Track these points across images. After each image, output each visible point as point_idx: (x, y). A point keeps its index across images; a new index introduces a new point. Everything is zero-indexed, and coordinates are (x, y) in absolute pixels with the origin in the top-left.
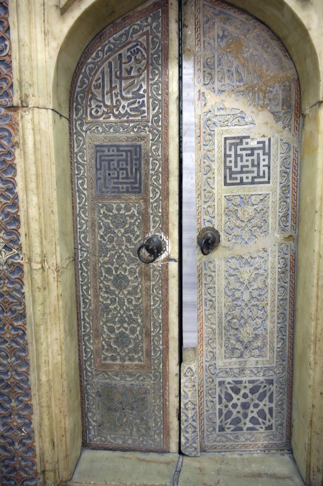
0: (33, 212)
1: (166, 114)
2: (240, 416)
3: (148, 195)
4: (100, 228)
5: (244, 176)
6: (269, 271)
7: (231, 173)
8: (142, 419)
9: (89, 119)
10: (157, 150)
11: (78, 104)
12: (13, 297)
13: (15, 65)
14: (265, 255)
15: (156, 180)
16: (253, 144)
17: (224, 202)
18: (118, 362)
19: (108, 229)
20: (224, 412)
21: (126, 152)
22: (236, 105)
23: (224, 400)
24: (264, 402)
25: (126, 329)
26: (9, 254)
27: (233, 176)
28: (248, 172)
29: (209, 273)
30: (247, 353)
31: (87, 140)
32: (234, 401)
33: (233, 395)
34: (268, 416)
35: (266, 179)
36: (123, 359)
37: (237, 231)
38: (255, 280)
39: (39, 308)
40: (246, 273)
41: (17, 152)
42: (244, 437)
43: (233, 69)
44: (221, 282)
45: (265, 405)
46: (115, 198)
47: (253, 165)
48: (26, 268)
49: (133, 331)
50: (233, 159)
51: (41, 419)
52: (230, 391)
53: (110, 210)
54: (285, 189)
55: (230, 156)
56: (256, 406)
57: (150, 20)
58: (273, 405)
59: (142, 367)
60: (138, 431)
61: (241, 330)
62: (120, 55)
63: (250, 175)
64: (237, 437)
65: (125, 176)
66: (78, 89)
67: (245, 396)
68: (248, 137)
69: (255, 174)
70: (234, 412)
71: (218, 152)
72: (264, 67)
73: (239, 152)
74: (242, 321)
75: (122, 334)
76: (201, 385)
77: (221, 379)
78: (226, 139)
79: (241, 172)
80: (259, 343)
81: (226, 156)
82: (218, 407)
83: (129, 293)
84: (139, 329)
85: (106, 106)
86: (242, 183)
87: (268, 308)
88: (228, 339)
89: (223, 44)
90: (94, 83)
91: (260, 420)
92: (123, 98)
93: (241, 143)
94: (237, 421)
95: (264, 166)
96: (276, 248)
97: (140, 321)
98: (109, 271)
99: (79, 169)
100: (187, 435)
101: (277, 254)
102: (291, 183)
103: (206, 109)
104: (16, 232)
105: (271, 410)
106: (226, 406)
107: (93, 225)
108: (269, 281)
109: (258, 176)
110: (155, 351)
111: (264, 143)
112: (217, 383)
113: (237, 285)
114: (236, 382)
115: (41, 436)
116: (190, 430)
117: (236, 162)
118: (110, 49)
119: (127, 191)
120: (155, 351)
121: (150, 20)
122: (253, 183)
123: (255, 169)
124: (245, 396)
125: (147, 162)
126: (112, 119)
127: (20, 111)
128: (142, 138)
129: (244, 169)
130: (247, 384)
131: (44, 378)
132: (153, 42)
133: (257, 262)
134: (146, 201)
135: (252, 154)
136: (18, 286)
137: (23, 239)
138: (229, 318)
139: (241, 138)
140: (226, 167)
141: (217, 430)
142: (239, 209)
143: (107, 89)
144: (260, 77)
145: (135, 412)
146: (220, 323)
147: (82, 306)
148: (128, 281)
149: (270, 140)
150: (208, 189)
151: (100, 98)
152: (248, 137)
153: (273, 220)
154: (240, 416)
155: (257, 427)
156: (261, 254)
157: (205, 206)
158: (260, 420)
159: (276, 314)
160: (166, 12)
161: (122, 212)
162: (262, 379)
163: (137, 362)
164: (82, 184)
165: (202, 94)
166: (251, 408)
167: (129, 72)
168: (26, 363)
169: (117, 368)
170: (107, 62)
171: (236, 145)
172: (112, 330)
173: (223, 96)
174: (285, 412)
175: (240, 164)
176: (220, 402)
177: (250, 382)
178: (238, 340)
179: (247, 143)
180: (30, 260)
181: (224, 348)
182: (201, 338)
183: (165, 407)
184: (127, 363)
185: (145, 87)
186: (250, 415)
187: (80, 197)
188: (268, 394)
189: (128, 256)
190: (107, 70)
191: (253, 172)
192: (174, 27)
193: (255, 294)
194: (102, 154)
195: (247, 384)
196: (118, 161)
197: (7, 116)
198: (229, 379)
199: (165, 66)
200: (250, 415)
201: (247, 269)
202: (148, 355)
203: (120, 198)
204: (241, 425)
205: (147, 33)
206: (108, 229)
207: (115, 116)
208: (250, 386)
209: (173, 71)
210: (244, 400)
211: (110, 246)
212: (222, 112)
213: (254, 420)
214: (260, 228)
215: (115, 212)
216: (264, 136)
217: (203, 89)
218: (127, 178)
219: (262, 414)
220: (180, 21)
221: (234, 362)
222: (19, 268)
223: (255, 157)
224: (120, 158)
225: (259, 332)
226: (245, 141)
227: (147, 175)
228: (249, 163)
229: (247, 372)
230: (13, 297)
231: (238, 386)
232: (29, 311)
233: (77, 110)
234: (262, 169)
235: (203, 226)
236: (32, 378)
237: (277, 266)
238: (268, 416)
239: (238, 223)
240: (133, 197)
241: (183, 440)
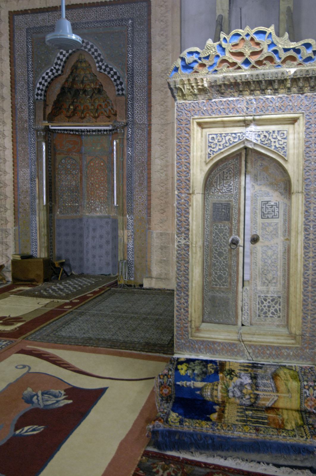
0: (194, 227)
1: (240, 193)
2: (267, 311)
3: (232, 221)
4: (213, 233)
5: (269, 215)
6: (279, 252)
7: (264, 214)
8: (227, 311)
9: (211, 193)
10: (236, 205)
11: (208, 188)
12: (185, 256)
13: (191, 181)
14: (277, 245)
15: (236, 216)
16: (272, 204)
17: (261, 224)
18: (218, 286)
19: (217, 234)
20: (260, 308)
21: (225, 205)
22: (266, 189)
23: (260, 304)
24: (277, 306)
25: (222, 273)
26: (185, 241)
29: (255, 252)
30: (270, 285)
31: (210, 201)
32: (265, 304)
33: (264, 302)
34: (279, 312)
35: (277, 217)
36: (220, 285)
37: (266, 236)
38: (273, 255)
39: (194, 260)
40: (270, 253)
41: (190, 208)
42: (269, 320)
43: (265, 177)
44: (259, 256)
45: (277, 307)
46: (220, 222)
47: (272, 211)
48: (190, 246)
49: (224, 274)
50: (264, 209)
51: (192, 300)
52: (263, 300)
53: (217, 227)
54: (285, 221)
55: (263, 208)
56: (274, 307)
57: (235, 160)
58: (281, 307)
59: (228, 289)
60: (225, 316)
61: (268, 275)
62: (224, 172)
63: (271, 215)
64: (265, 320)
66: (208, 183)
67: (269, 302)
68: (270, 201)
70: (264, 309)
71: (259, 206)
72: (277, 176)
73: (267, 207)
74: (268, 272)
75: (220, 275)
76: (251, 297)
77: (259, 295)
78: (262, 202)
79: (268, 214)
80: (275, 281)
81: (262, 208)
82: (258, 306)
83: (224, 259)
84: (227, 273)
85: (218, 189)
86: (268, 218)
87: (279, 267)
88: (262, 278)
89: (261, 168)
90: (214, 181)
91: (275, 313)
92: (224, 186)
93: (268, 203)
94: (265, 313)
96: (282, 243)
97: (227, 270)
98: (216, 250)
99: (207, 211)
100: (245, 317)
101: (282, 245)
102: (287, 219)
103: (255, 191)
104: (188, 234)
105: (280, 309)
106: (261, 306)
107: (211, 232)
108: (279, 256)
109: (275, 216)
110: (233, 282)
111: (276, 203)
112: (257, 296)
113: (266, 257)
114: (265, 296)
115: (191, 307)
116: (246, 314)
118: (220, 170)
119: (225, 220)
120: (233, 282)
121: (235, 160)
122: (272, 218)
123: (273, 213)
124: (269, 302)
125: (232, 210)
126: (220, 194)
127: (192, 195)
128: (231, 201)
130: (270, 298)
131: (194, 285)
132: (236, 167)
133: (274, 248)
134: (231, 224)
135: (272, 207)
136: (187, 252)
137: (190, 236)
138: (263, 270)
139: (268, 202)
140: (262, 212)
141: (257, 316)
142: (267, 227)
143: (218, 183)
144: (275, 180)
145: (224, 308)
146: (259, 272)
147: (205, 263)
148: (223, 254)
149: (279, 202)
150: (255, 220)
151: (215, 186)
152: (270, 201)
153: (280, 232)
154: (267, 311)
155: (274, 316)
156: (276, 245)
157: (254, 226)
158: (275, 313)
159: (281, 269)
160: (241, 158)
161: (222, 227)
162: (276, 296)
163: (225, 287)
164: (207, 217)
165: (253, 186)
166: (272, 308)
167: (227, 178)
168: (188, 279)
169: (217, 289)
170: (219, 174)
171: (266, 204)
172: (216, 273)
173: (261, 187)
174: (286, 311)
175: (267, 211)
176: (259, 304)
177: (271, 297)
178: (266, 279)
180: (192, 243)
181: (260, 282)
182: (251, 277)
183: (236, 306)
184: (222, 287)
185: (232, 183)
186: (271, 311)
187: (207, 222)
188: (279, 302)
189: (224, 244)
190: (219, 177)
192: (243, 163)
193: (273, 261)
195: (270, 298)
196: (222, 209)
197: (188, 196)
198: (263, 295)
199: (240, 175)
200: (271, 311)
201: (270, 251)
202: (230, 284)
203: (221, 222)
204: (267, 315)
205: (233, 165)
206: (217, 234)
207: (221, 193)
208: (271, 298)
209: (243, 178)
210: (268, 304)
211: (217, 240)
212: (261, 192)
213: (273, 313)
214: (275, 235)
215: (219, 227)
216: (277, 201)
217: (254, 184)
218: (225, 215)
219: (276, 310)
220: (246, 162)
221: (264, 288)
222: (188, 246)
223: (273, 209)
225: (275, 276)
226: (269, 202)
227: (232, 214)
228: (271, 211)
229: (270, 292)
230: (185, 256)
231: (266, 298)
232: (190, 261)
233: (207, 190)
235: (253, 234)
236: (190, 285)
237: (282, 250)
238: (279, 312)
239: (267, 233)
240: (227, 222)
241: (243, 319)
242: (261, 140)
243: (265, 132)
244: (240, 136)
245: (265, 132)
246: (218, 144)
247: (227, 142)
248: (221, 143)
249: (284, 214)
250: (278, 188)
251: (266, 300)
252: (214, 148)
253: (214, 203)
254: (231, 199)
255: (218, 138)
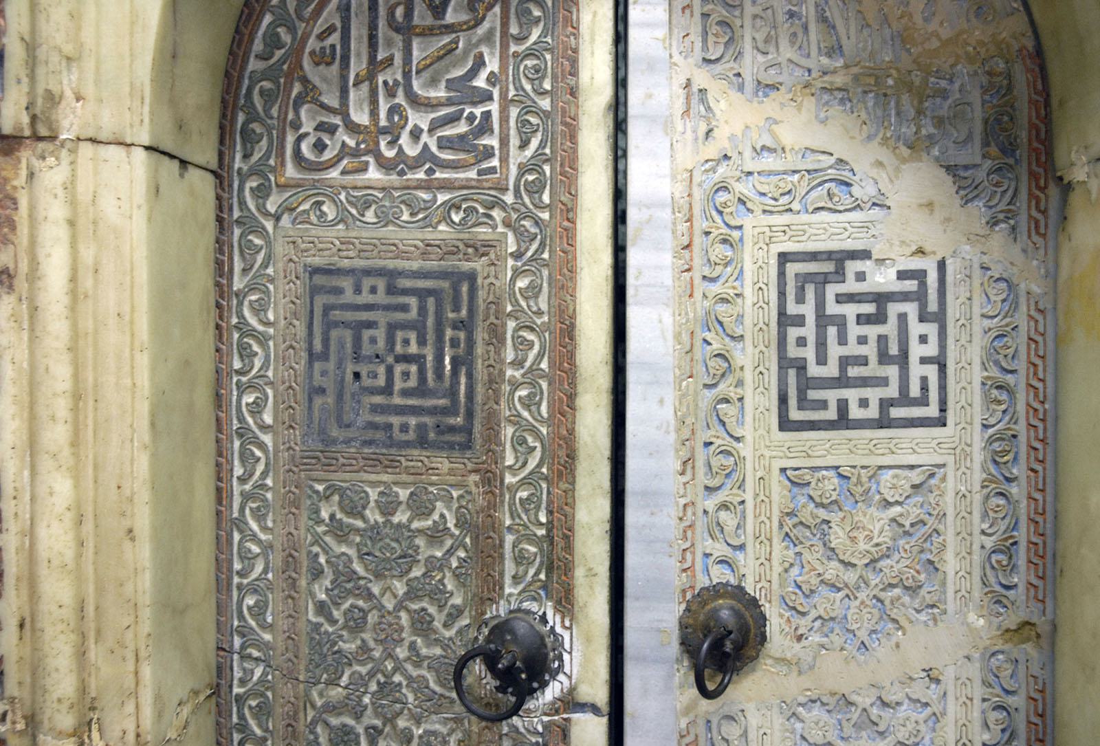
3: (498, 458)
4: (317, 573)
5: (852, 395)
7: (806, 383)
9: (291, 171)
10: (533, 292)
11: (253, 117)
14: (933, 693)
15: (528, 403)
16: (883, 279)
17: (778, 489)
19: (345, 581)
21: (422, 294)
22: (820, 138)
27: (813, 395)
28: (864, 382)
31: (280, 249)
35: (932, 411)
46: (375, 463)
47: (884, 358)
50: (809, 331)
53: (356, 511)
55: (800, 321)
63: (874, 395)
65: (413, 383)
66: (253, 65)
68: (865, 255)
69: (892, 391)
73: (832, 308)
78: (784, 258)
79: (842, 381)
81: (785, 320)
85: (352, 128)
86: (843, 421)
90: (312, 44)
92: (414, 100)
93: (840, 275)
95: (924, 361)
96: (974, 671)
99: (246, 353)
101: (978, 691)
102: (1021, 428)
107: (290, 561)
109: (904, 399)
111: (920, 275)
117: (821, 345)
119: (422, 442)
122: (883, 422)
123: (892, 372)
125: (497, 336)
126: (374, 174)
128: (482, 249)
129: (853, 372)
134: (491, 479)
135: (879, 318)
139: (840, 259)
140: (785, 362)
142: (835, 517)
143: (357, 66)
149: (942, 265)
150: (722, 441)
151: (332, 100)
152: (865, 255)
156: (919, 690)
157: (711, 503)
161: (401, 517)
164: (257, 408)
165: (695, 97)
171: (822, 281)
173: (771, 105)
175: (835, 351)
179: (861, 277)
185: (492, 65)
187: (245, 457)
189: (418, 685)
191: (884, 382)
194: (332, 299)
196: (392, 328)
203: (391, 465)
206: (345, 581)
207: (385, 165)
211: (350, 646)
212: (769, 162)
214: (913, 590)
215: (374, 516)
216: (921, 252)
217: (702, 78)
218: (421, 390)
223: (890, 328)
224: (399, 316)
226: (852, 267)
227: (494, 382)
228: (870, 350)
233: (249, 139)
234: (917, 371)
235: (702, 581)
239: (832, 570)
240: (443, 463)
249: (997, 389)
250: (928, 129)
253: (315, 271)
254: (483, 232)
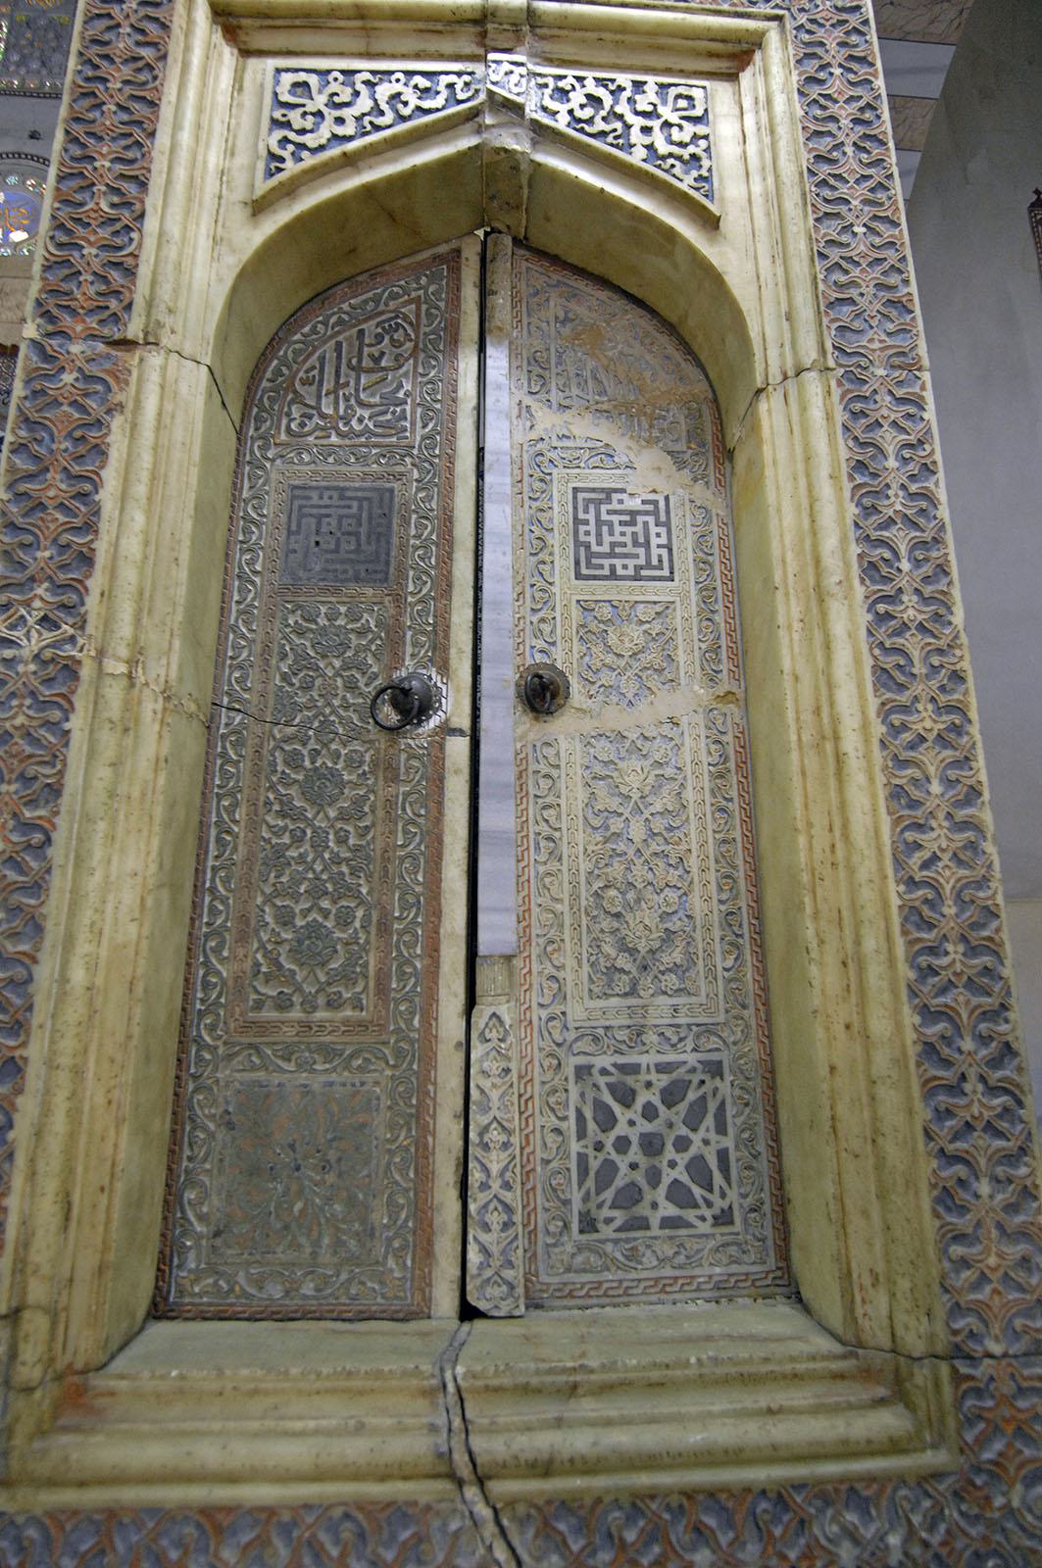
242: (571, 112)
243: (590, 83)
244: (459, 87)
245: (590, 83)
246: (330, 114)
247: (384, 106)
248: (346, 113)
251: (626, 1097)
252: (302, 132)
255: (334, 87)
